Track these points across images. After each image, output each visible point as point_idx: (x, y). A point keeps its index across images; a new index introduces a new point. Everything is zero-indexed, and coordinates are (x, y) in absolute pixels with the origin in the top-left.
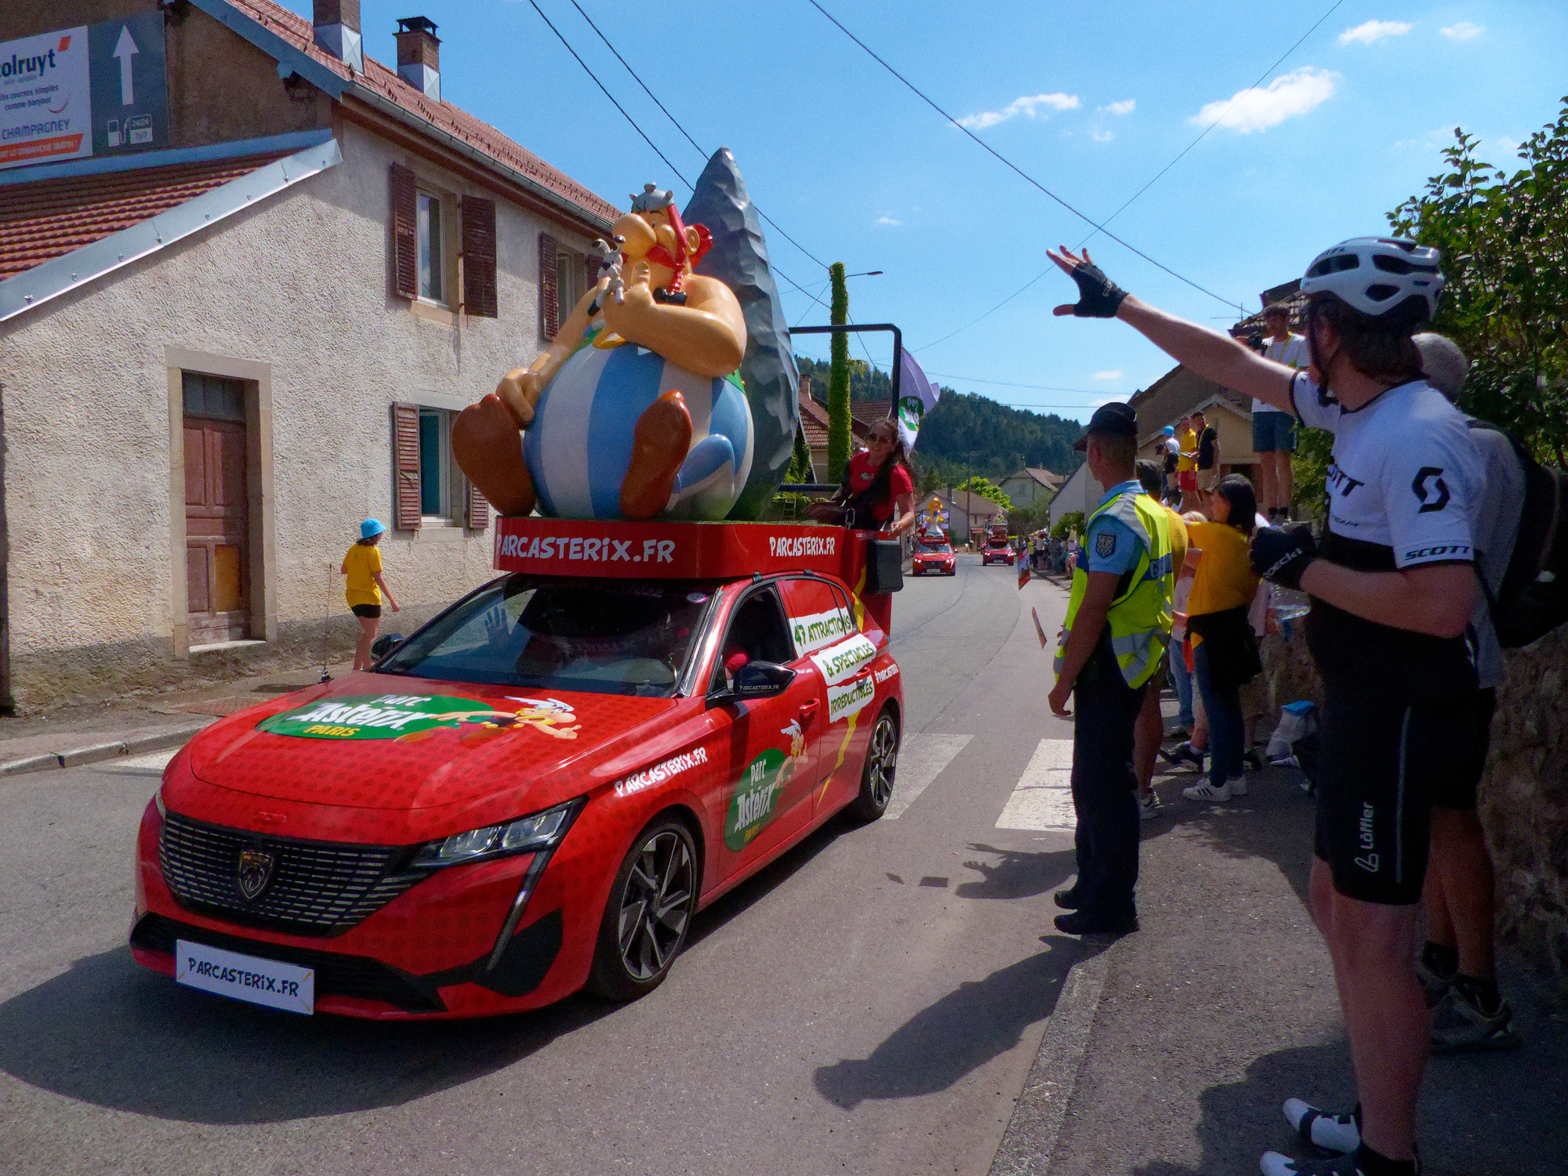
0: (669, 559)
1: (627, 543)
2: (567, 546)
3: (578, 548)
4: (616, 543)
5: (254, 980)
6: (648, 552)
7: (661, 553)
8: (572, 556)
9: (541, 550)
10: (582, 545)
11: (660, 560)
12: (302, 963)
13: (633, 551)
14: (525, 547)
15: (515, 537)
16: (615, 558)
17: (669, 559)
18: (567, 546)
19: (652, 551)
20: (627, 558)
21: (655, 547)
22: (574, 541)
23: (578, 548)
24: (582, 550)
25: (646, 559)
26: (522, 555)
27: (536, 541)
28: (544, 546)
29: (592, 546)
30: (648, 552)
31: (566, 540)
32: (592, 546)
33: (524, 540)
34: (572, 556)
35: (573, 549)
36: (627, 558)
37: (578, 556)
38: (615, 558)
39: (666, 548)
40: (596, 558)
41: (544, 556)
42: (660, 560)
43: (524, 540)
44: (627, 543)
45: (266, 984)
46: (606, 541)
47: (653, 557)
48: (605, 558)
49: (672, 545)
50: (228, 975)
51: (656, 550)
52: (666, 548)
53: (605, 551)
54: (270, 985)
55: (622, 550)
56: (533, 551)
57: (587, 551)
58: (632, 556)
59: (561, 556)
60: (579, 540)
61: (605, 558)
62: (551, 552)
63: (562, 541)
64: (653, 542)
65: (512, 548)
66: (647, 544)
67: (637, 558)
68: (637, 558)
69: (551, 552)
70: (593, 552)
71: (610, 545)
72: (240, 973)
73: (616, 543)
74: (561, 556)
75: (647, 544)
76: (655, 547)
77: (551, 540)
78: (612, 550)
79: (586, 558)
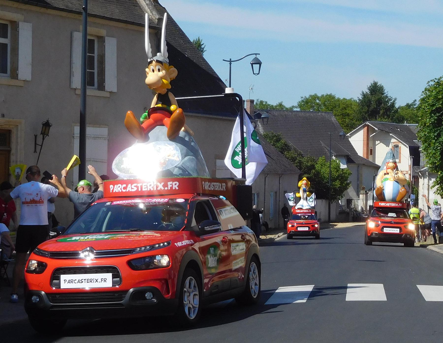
0: (177, 188)
5: (91, 281)
9: (132, 188)
11: (174, 188)
12: (108, 272)
14: (125, 188)
15: (120, 185)
19: (171, 186)
21: (172, 184)
23: (146, 187)
24: (147, 187)
25: (169, 189)
26: (124, 191)
27: (130, 185)
28: (133, 187)
30: (170, 186)
33: (125, 185)
34: (144, 190)
36: (163, 188)
37: (146, 189)
39: (176, 184)
40: (152, 189)
41: (133, 190)
42: (174, 188)
43: (125, 185)
49: (178, 183)
51: (172, 186)
52: (176, 184)
54: (97, 281)
56: (129, 189)
58: (164, 188)
59: (140, 190)
64: (171, 183)
65: (119, 189)
67: (166, 188)
68: (166, 188)
74: (140, 190)
76: (172, 184)
79: (149, 190)
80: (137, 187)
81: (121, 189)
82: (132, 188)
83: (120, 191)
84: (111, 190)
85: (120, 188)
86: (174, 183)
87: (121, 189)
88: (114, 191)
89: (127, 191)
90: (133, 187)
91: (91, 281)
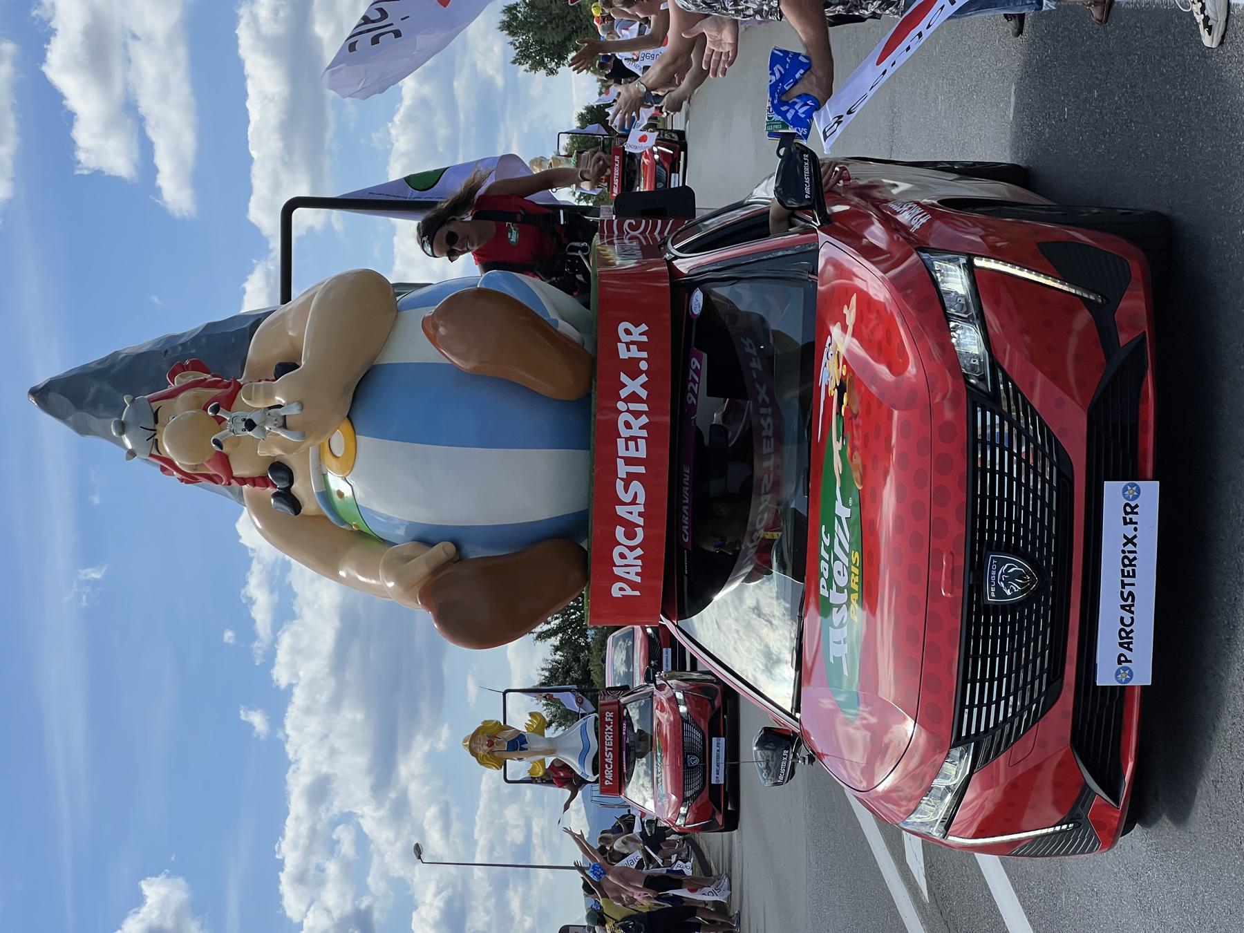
0: (644, 327)
1: (624, 378)
2: (629, 461)
3: (631, 444)
4: (624, 393)
5: (1129, 562)
6: (635, 353)
7: (636, 337)
8: (642, 453)
9: (633, 502)
10: (627, 439)
13: (632, 369)
14: (630, 535)
15: (617, 551)
16: (643, 394)
17: (644, 327)
18: (629, 461)
20: (643, 378)
21: (628, 344)
22: (622, 451)
24: (634, 439)
25: (644, 355)
26: (640, 531)
27: (621, 511)
28: (627, 498)
29: (628, 425)
30: (635, 353)
31: (620, 462)
32: (628, 425)
33: (620, 531)
34: (642, 453)
35: (632, 453)
36: (643, 378)
37: (642, 443)
38: (643, 394)
39: (628, 332)
40: (644, 420)
41: (641, 499)
43: (620, 531)
44: (624, 378)
45: (1130, 547)
46: (621, 406)
47: (641, 346)
48: (644, 407)
49: (624, 325)
51: (633, 343)
52: (628, 332)
53: (633, 406)
55: (633, 385)
56: (632, 513)
57: (635, 432)
58: (642, 372)
59: (642, 470)
60: (621, 443)
61: (644, 407)
63: (623, 469)
64: (621, 347)
66: (623, 354)
67: (644, 366)
68: (644, 366)
69: (636, 486)
70: (637, 423)
71: (626, 400)
72: (1123, 585)
73: (624, 393)
74: (642, 470)
75: (623, 354)
76: (628, 344)
77: (620, 485)
78: (634, 398)
79: (644, 433)
80: (631, 477)
81: (632, 549)
82: (633, 502)
83: (639, 552)
84: (629, 592)
86: (624, 337)
87: (632, 549)
88: (638, 579)
89: (641, 521)
90: (627, 498)
91: (1129, 562)
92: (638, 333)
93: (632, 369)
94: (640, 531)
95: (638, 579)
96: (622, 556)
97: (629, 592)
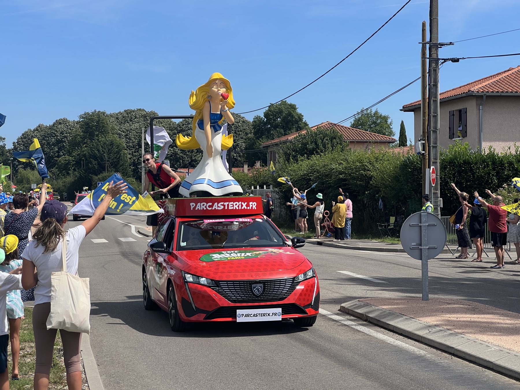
1: (246, 203)
2: (228, 205)
6: (251, 206)
8: (230, 208)
9: (218, 207)
13: (248, 205)
14: (209, 206)
15: (205, 204)
16: (243, 208)
18: (228, 205)
20: (246, 208)
22: (230, 203)
24: (233, 206)
26: (211, 208)
27: (216, 204)
29: (236, 204)
31: (228, 203)
32: (236, 204)
33: (211, 204)
34: (230, 208)
35: (230, 206)
37: (232, 208)
38: (243, 208)
40: (237, 208)
41: (219, 209)
43: (211, 204)
44: (246, 203)
46: (240, 203)
47: (252, 207)
50: (247, 316)
53: (240, 206)
55: (244, 205)
56: (215, 206)
57: (235, 206)
59: (226, 208)
60: (232, 203)
62: (222, 207)
63: (226, 204)
66: (251, 203)
67: (248, 208)
68: (248, 208)
69: (222, 207)
70: (237, 206)
71: (241, 204)
73: (243, 203)
74: (226, 208)
75: (251, 203)
77: (222, 203)
78: (242, 206)
80: (224, 206)
81: (206, 207)
82: (218, 207)
83: (205, 209)
84: (192, 207)
85: (205, 206)
87: (206, 207)
88: (196, 209)
89: (213, 209)
90: (219, 205)
92: (254, 207)
93: (248, 205)
94: (211, 208)
95: (196, 209)
96: (203, 205)
97: (192, 207)
